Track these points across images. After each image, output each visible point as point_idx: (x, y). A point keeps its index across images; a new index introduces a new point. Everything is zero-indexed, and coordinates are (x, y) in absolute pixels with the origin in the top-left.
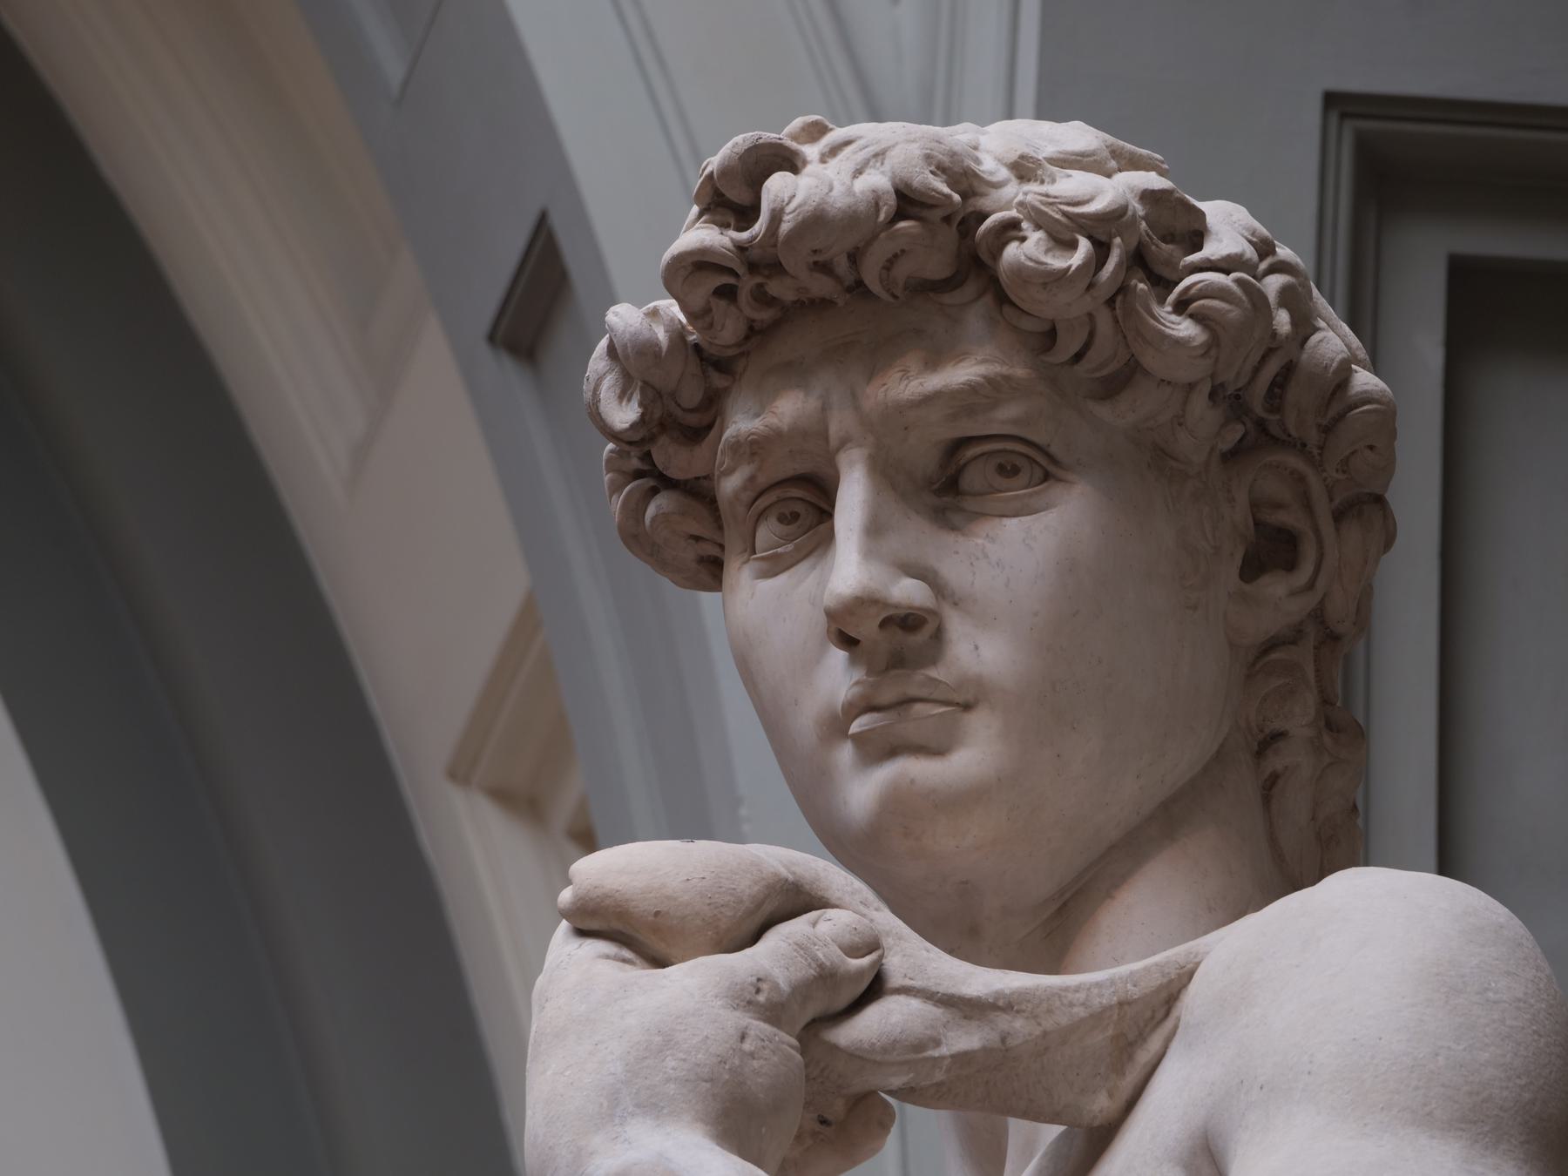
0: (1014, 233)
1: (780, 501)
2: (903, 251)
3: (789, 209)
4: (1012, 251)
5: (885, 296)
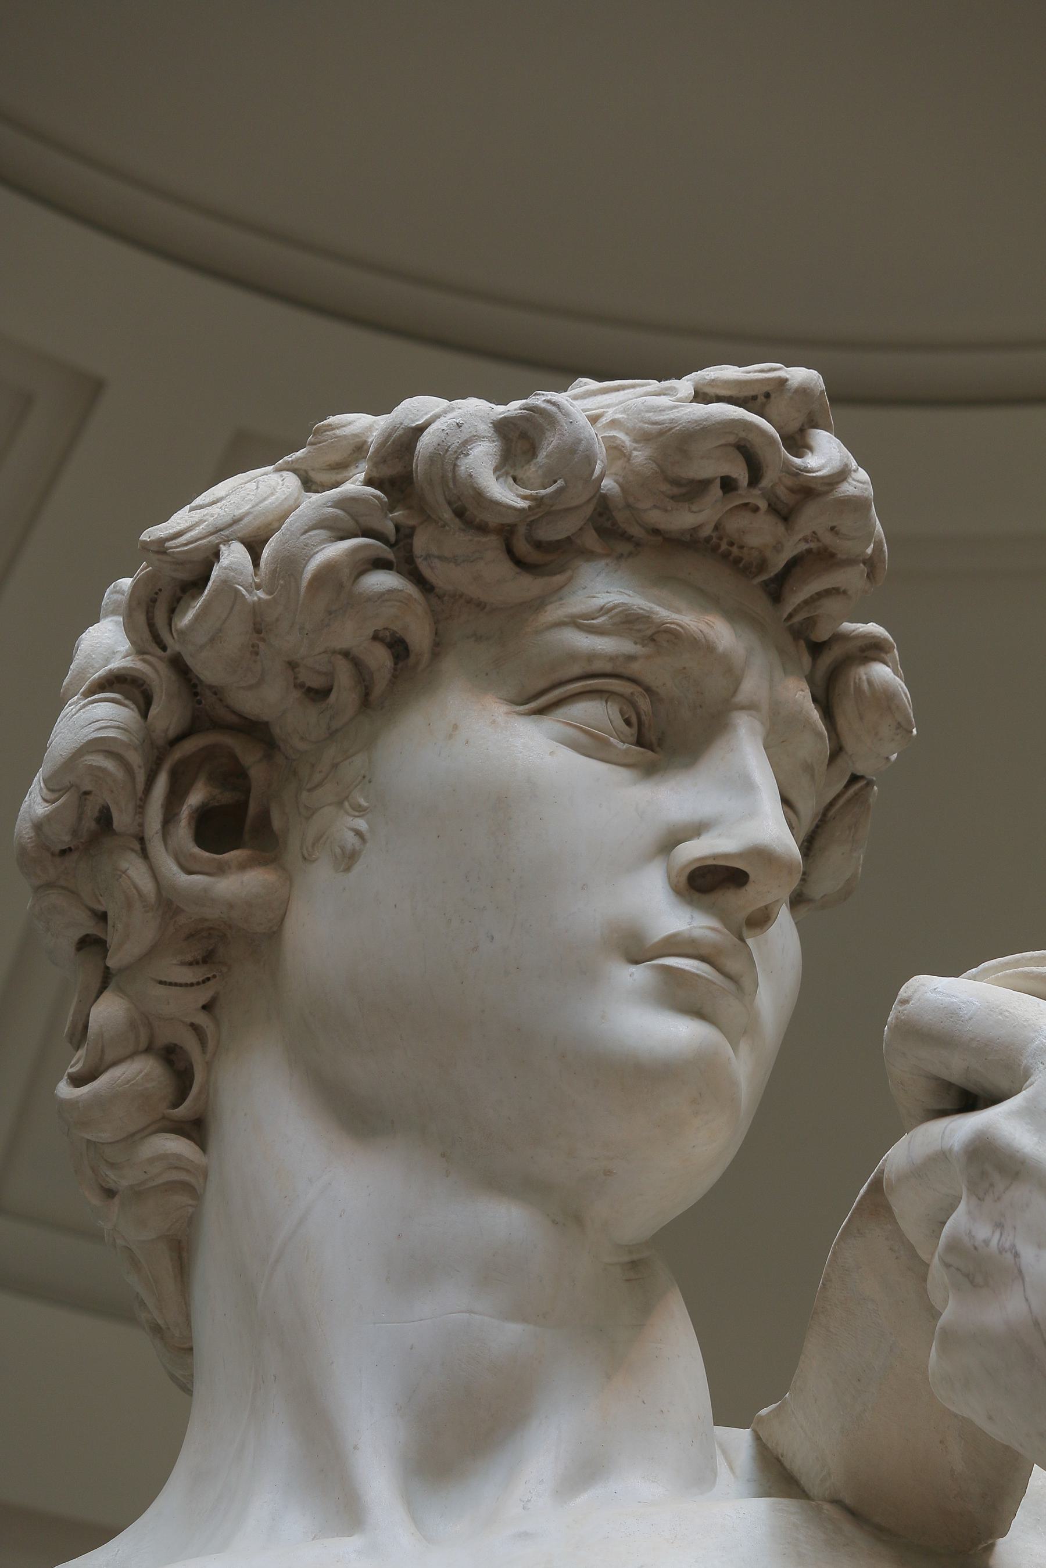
0: (883, 655)
2: (845, 592)
3: (854, 475)
4: (882, 672)
5: (789, 609)
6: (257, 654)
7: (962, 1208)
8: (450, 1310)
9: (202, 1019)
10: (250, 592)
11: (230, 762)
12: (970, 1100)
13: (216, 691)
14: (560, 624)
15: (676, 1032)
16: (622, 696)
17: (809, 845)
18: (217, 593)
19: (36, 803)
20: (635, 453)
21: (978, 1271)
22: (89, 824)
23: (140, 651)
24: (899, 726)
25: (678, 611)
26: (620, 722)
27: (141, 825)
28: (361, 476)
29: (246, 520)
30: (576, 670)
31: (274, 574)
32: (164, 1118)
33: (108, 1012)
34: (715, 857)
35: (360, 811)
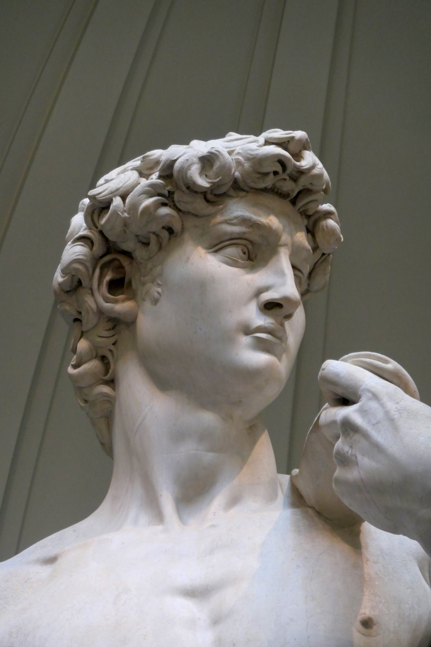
1: (245, 246)
3: (318, 166)
4: (331, 222)
6: (126, 232)
7: (340, 440)
8: (189, 449)
9: (112, 348)
10: (122, 213)
11: (122, 259)
12: (345, 402)
13: (114, 242)
14: (222, 223)
15: (260, 358)
16: (242, 245)
17: (303, 295)
18: (112, 215)
19: (59, 277)
20: (245, 164)
21: (345, 461)
22: (75, 283)
23: (89, 228)
24: (337, 240)
25: (260, 216)
26: (242, 254)
27: (91, 285)
28: (157, 174)
29: (121, 189)
30: (227, 237)
31: (130, 209)
32: (102, 379)
33: (83, 345)
34: (272, 299)
35: (159, 285)
